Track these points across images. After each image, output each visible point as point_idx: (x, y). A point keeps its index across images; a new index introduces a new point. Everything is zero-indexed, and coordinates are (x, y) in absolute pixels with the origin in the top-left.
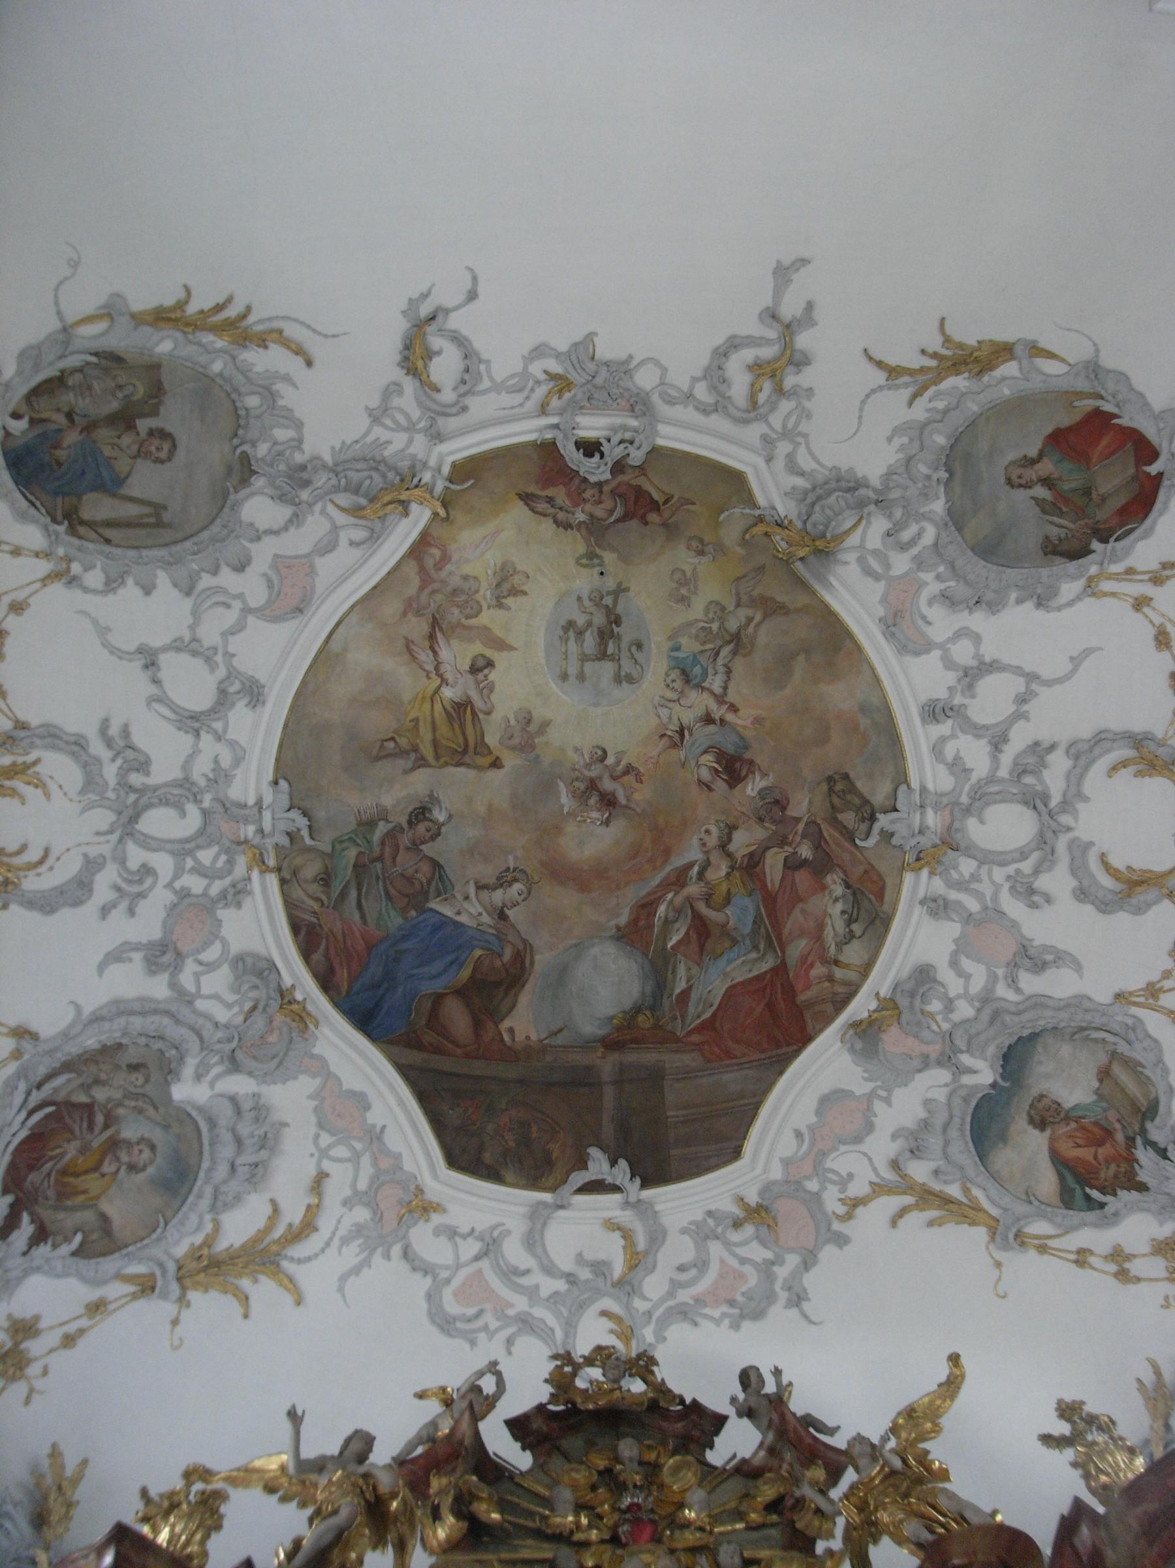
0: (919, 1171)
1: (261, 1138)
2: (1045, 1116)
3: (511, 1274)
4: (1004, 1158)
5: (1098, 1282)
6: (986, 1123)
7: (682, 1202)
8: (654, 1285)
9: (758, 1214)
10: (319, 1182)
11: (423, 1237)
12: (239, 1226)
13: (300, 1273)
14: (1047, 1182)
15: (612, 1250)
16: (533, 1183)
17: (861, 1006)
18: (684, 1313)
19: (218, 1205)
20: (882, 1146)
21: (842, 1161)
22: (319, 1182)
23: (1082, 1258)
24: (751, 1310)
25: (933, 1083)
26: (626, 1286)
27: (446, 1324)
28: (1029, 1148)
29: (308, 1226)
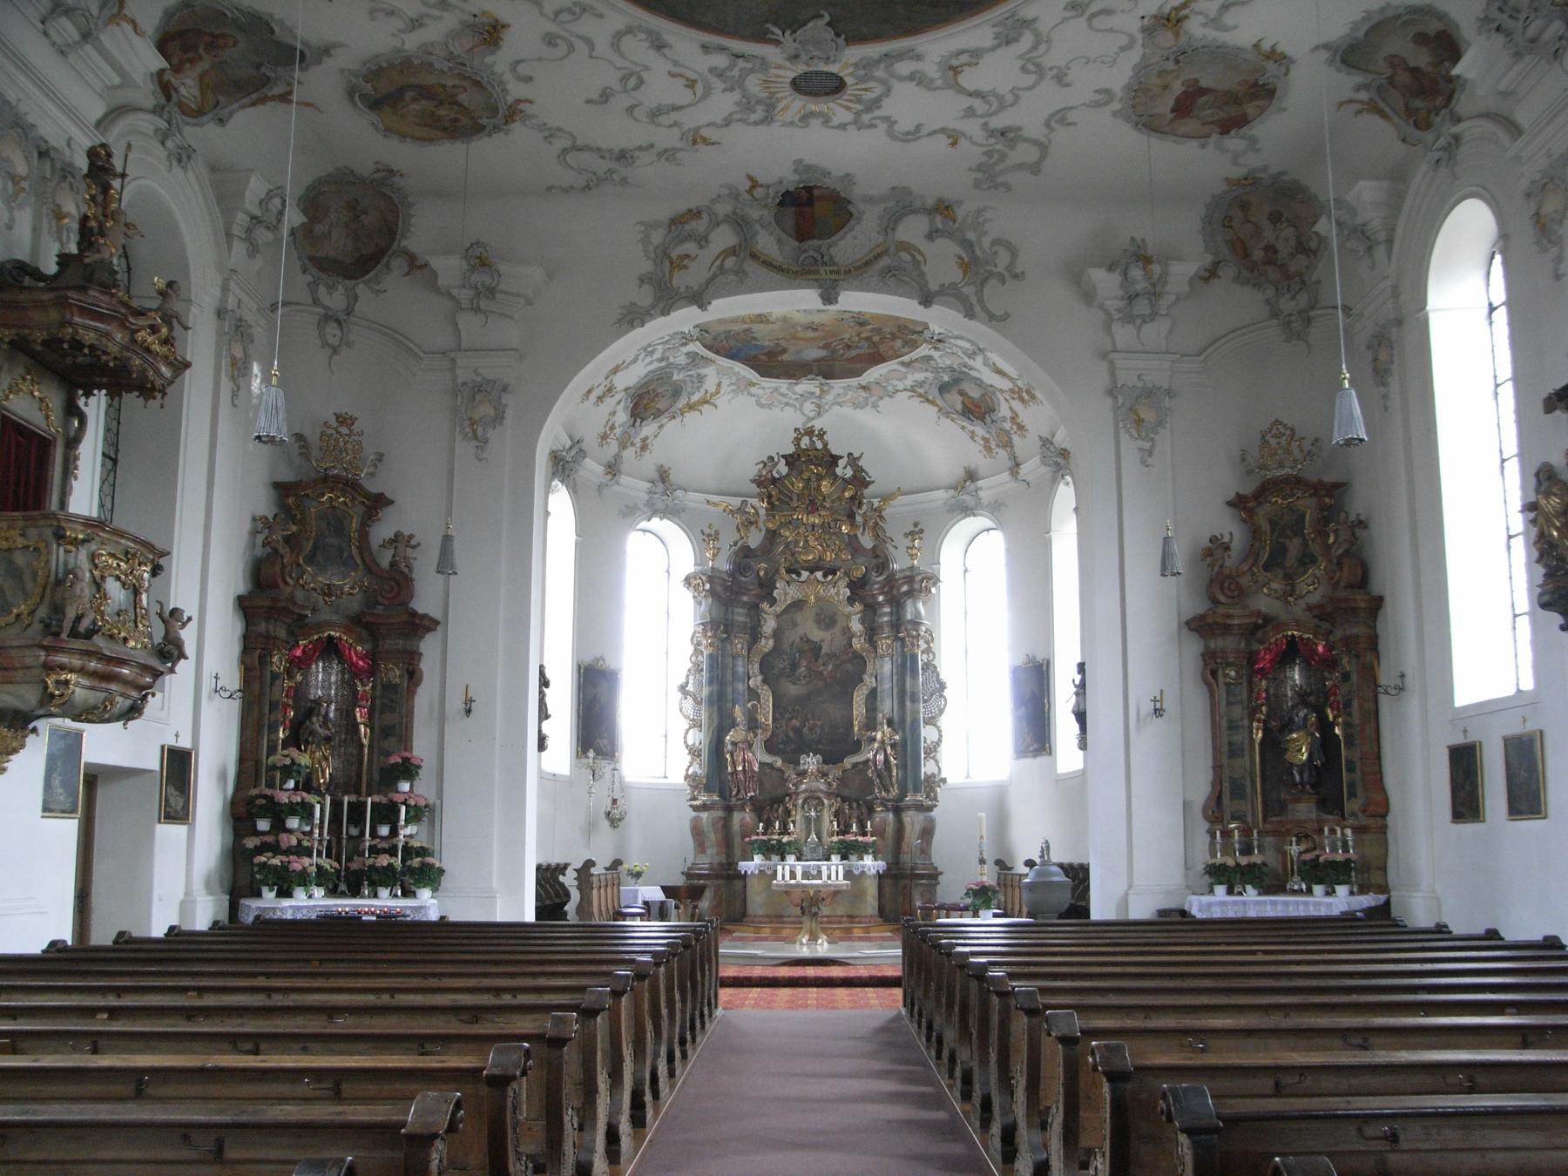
0: (921, 391)
1: (701, 379)
2: (962, 393)
3: (783, 395)
4: (947, 396)
5: (965, 437)
6: (943, 388)
7: (838, 385)
8: (829, 397)
9: (864, 388)
10: (719, 384)
11: (753, 390)
12: (694, 398)
13: (717, 402)
14: (959, 407)
15: (818, 392)
16: (790, 377)
17: (906, 359)
18: (840, 404)
19: (690, 394)
20: (909, 383)
21: (895, 382)
22: (719, 384)
23: (963, 428)
24: (856, 406)
25: (930, 375)
26: (819, 397)
27: (762, 406)
28: (957, 401)
29: (717, 392)
